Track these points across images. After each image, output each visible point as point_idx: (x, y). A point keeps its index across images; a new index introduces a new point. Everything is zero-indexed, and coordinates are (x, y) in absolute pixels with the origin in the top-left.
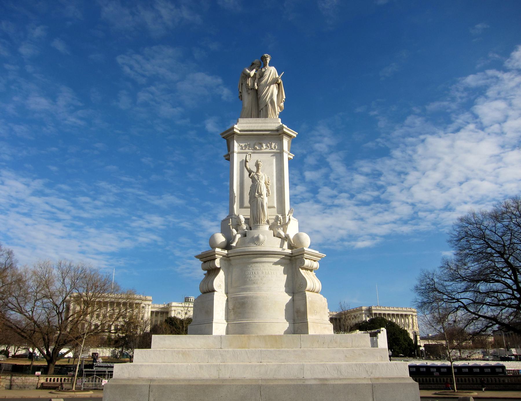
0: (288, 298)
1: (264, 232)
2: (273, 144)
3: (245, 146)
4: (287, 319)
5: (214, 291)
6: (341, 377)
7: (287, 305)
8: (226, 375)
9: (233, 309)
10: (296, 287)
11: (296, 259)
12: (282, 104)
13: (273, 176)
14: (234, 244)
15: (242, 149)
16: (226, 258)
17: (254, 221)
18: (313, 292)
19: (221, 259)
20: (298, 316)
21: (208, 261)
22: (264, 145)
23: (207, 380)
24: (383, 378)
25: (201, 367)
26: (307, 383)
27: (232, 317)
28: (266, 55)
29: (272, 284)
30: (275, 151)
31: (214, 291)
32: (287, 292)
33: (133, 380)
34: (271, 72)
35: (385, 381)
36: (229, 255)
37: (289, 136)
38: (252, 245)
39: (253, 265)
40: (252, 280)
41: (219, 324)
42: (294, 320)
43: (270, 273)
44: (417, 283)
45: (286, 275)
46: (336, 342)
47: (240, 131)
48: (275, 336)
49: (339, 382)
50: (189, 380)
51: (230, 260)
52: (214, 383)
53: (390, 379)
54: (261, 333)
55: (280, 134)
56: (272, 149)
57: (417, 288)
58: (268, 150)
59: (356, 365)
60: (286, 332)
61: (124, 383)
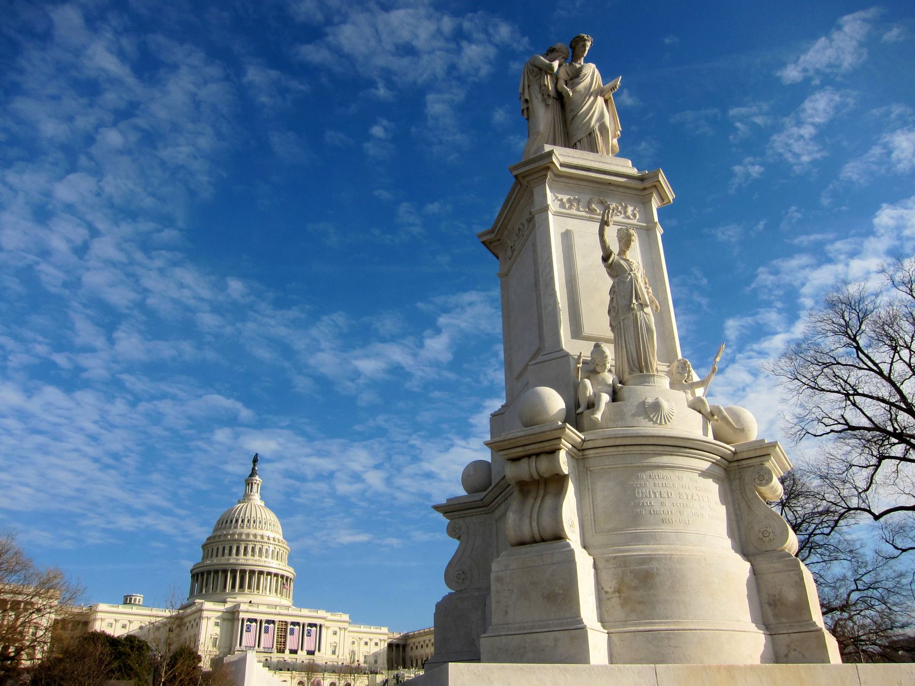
2: (630, 209)
3: (569, 201)
9: (619, 591)
11: (741, 469)
15: (562, 205)
16: (580, 453)
17: (637, 366)
20: (775, 615)
21: (529, 456)
27: (618, 613)
28: (585, 36)
30: (635, 222)
34: (591, 72)
36: (586, 445)
37: (662, 197)
40: (655, 513)
43: (696, 497)
47: (562, 165)
51: (584, 458)
55: (645, 189)
56: (629, 218)
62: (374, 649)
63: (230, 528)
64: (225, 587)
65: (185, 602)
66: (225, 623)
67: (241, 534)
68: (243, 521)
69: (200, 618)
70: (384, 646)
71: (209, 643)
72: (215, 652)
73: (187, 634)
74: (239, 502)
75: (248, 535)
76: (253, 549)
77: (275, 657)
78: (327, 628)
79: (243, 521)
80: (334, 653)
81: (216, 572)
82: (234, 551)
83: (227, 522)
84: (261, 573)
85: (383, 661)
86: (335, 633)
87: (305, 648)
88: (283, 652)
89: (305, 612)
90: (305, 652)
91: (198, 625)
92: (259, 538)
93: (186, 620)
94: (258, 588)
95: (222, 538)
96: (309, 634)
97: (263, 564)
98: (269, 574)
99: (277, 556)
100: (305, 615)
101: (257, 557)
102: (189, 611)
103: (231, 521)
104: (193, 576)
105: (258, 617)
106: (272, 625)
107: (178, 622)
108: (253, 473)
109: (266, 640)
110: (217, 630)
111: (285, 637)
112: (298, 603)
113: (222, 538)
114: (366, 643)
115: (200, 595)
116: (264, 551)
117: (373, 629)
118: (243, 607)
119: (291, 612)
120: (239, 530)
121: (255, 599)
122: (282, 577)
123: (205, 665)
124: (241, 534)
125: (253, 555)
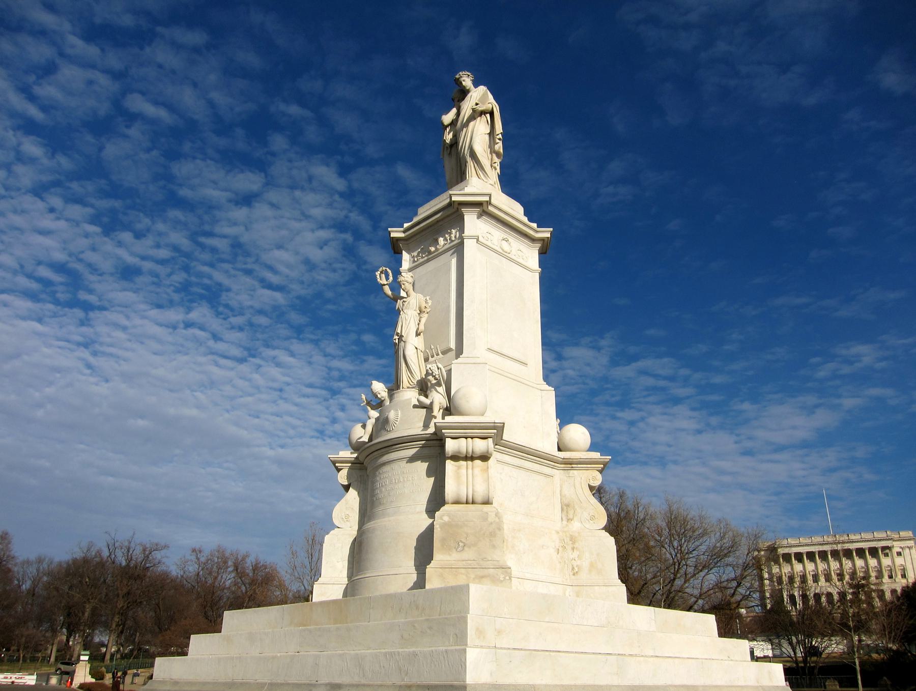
3: (418, 255)
5: (334, 527)
12: (499, 146)
13: (449, 291)
18: (473, 503)
19: (350, 468)
28: (457, 76)
34: (479, 96)
38: (383, 432)
41: (330, 584)
45: (432, 479)
56: (452, 241)
58: (447, 246)
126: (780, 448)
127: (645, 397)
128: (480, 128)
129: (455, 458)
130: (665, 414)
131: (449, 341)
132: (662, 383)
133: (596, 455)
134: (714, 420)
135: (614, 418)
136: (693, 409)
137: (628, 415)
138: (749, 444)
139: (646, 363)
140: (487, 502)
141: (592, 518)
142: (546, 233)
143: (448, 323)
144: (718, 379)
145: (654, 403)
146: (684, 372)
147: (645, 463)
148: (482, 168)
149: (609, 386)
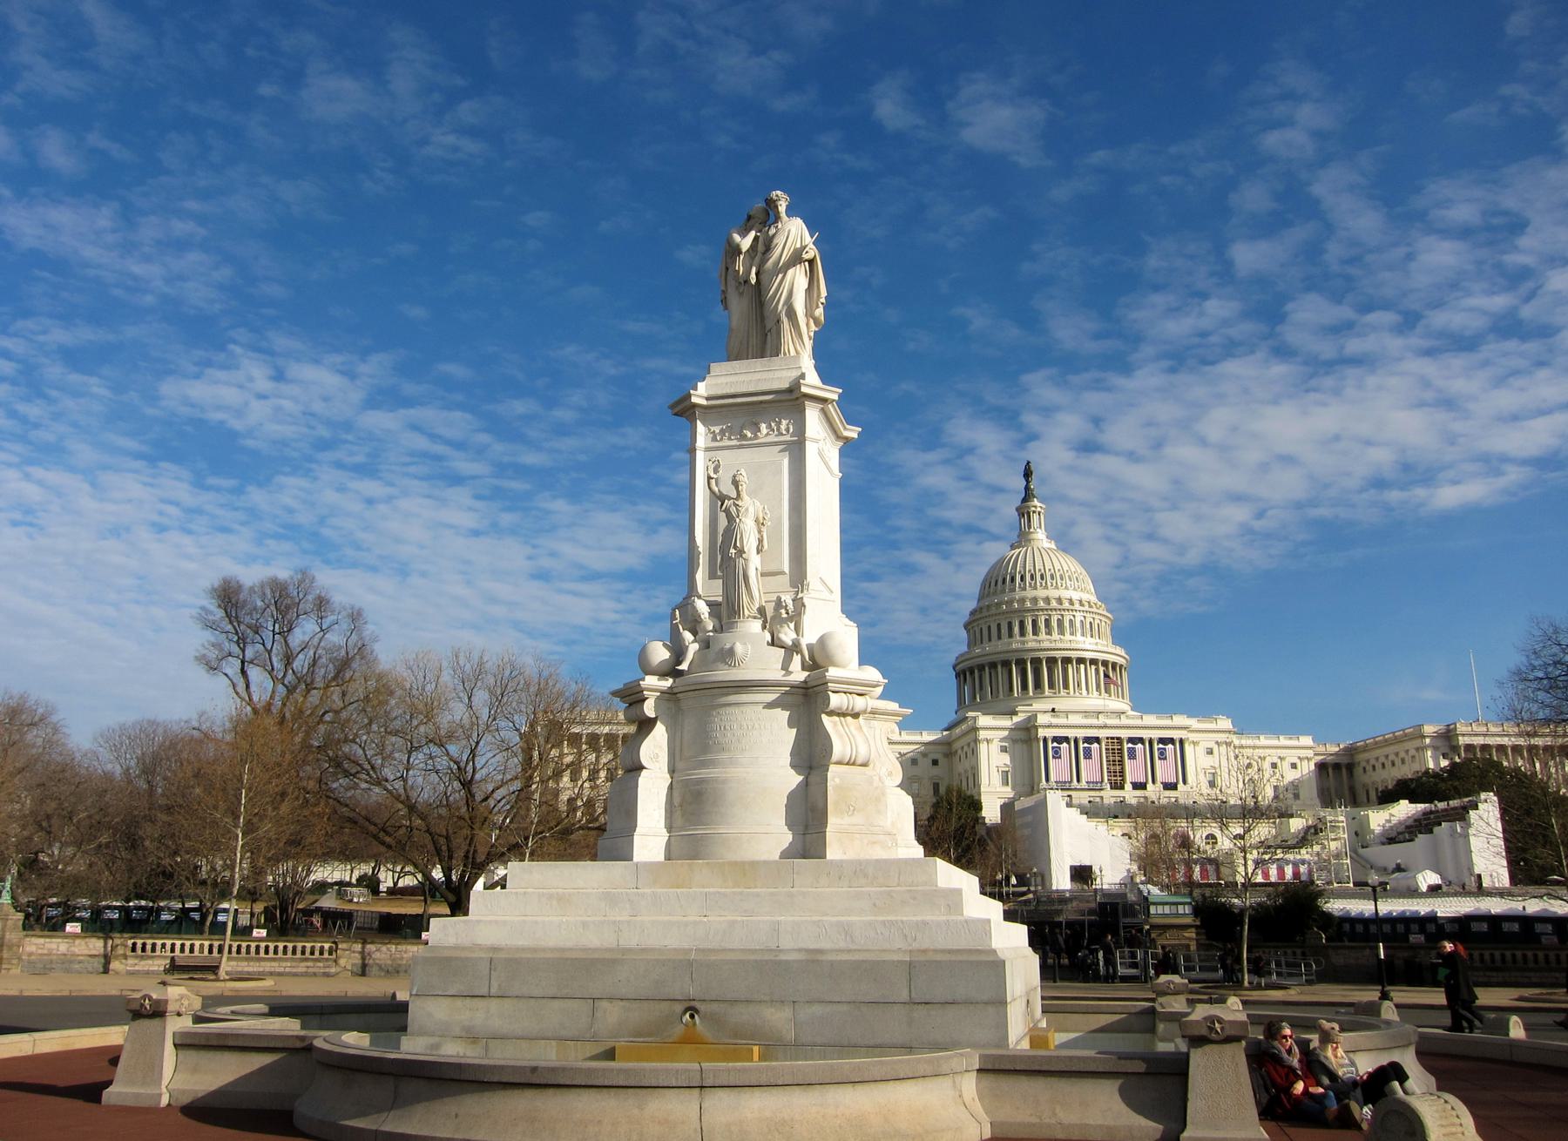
0: (796, 779)
1: (749, 638)
2: (784, 422)
3: (722, 432)
4: (790, 824)
5: (642, 768)
6: (852, 947)
7: (792, 796)
8: (631, 940)
10: (812, 756)
12: (819, 312)
14: (684, 666)
15: (714, 439)
17: (727, 612)
22: (763, 426)
23: (595, 950)
24: (935, 951)
25: (585, 925)
26: (783, 957)
27: (679, 821)
29: (762, 749)
30: (788, 438)
31: (641, 768)
32: (793, 766)
33: (464, 949)
34: (793, 233)
35: (939, 957)
38: (721, 666)
39: (722, 711)
41: (650, 835)
42: (806, 827)
44: (1518, 660)
46: (866, 876)
47: (707, 399)
48: (743, 863)
49: (845, 957)
50: (563, 950)
52: (607, 956)
53: (950, 951)
54: (732, 856)
57: (1521, 676)
59: (883, 922)
60: (786, 854)
61: (447, 954)
62: (1291, 776)
63: (1003, 591)
64: (1011, 689)
65: (952, 717)
66: (1019, 746)
67: (1022, 601)
68: (1022, 578)
69: (976, 741)
70: (1308, 768)
71: (997, 779)
72: (1008, 792)
73: (961, 767)
74: (1013, 547)
75: (1035, 600)
76: (1048, 622)
77: (1109, 796)
78: (1195, 743)
79: (1022, 578)
80: (1212, 784)
81: (993, 665)
82: (1016, 629)
83: (998, 581)
84: (1067, 660)
85: (1310, 792)
86: (1210, 752)
87: (1159, 778)
88: (1122, 788)
89: (1150, 720)
90: (1159, 786)
91: (975, 752)
92: (1054, 604)
93: (957, 746)
94: (1066, 686)
95: (993, 611)
96: (1163, 756)
97: (1068, 646)
98: (1081, 661)
99: (1092, 630)
100: (1152, 725)
101: (1055, 636)
102: (958, 731)
103: (1004, 581)
104: (957, 676)
105: (1071, 733)
106: (1096, 745)
107: (944, 749)
108: (1028, 495)
109: (1089, 770)
110: (1006, 759)
111: (1121, 762)
112: (1140, 705)
113: (993, 611)
114: (1274, 766)
115: (974, 706)
116: (1067, 624)
117: (1283, 741)
118: (1042, 719)
119: (1124, 721)
120: (1018, 594)
121: (1061, 704)
122: (1105, 663)
123: (991, 812)
124: (1022, 601)
125: (1049, 633)
126: (592, 576)
127: (405, 464)
128: (798, 278)
129: (831, 713)
130: (429, 497)
131: (782, 562)
132: (440, 449)
133: (893, 706)
134: (507, 519)
135: (341, 489)
136: (478, 497)
137: (371, 487)
138: (546, 562)
139: (426, 414)
140: (865, 765)
141: (890, 774)
142: (852, 432)
143: (781, 539)
144: (531, 458)
145: (416, 477)
146: (484, 438)
147: (374, 569)
148: (800, 336)
149: (350, 437)
